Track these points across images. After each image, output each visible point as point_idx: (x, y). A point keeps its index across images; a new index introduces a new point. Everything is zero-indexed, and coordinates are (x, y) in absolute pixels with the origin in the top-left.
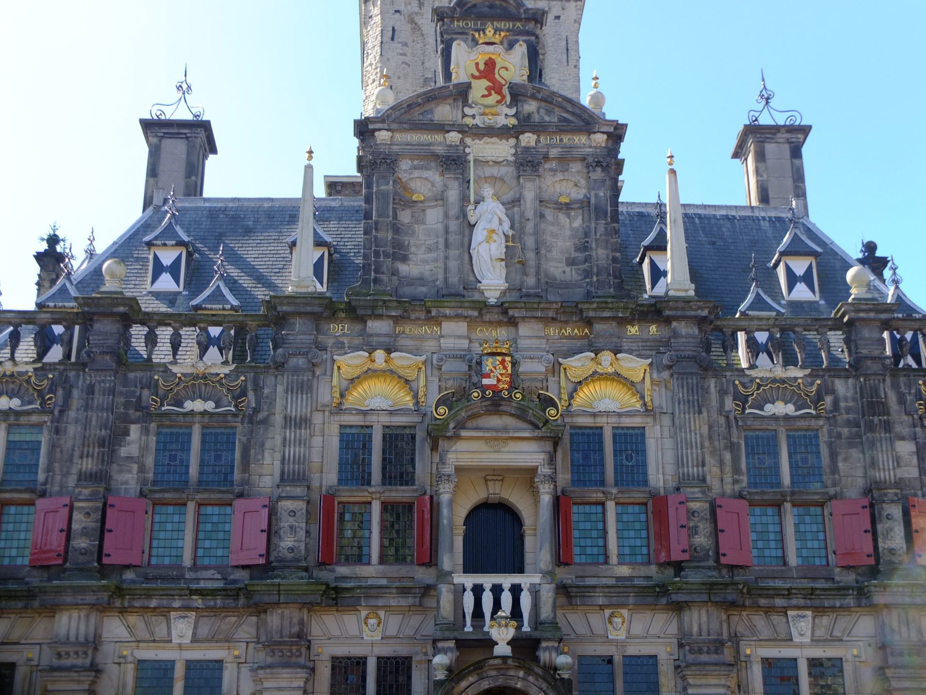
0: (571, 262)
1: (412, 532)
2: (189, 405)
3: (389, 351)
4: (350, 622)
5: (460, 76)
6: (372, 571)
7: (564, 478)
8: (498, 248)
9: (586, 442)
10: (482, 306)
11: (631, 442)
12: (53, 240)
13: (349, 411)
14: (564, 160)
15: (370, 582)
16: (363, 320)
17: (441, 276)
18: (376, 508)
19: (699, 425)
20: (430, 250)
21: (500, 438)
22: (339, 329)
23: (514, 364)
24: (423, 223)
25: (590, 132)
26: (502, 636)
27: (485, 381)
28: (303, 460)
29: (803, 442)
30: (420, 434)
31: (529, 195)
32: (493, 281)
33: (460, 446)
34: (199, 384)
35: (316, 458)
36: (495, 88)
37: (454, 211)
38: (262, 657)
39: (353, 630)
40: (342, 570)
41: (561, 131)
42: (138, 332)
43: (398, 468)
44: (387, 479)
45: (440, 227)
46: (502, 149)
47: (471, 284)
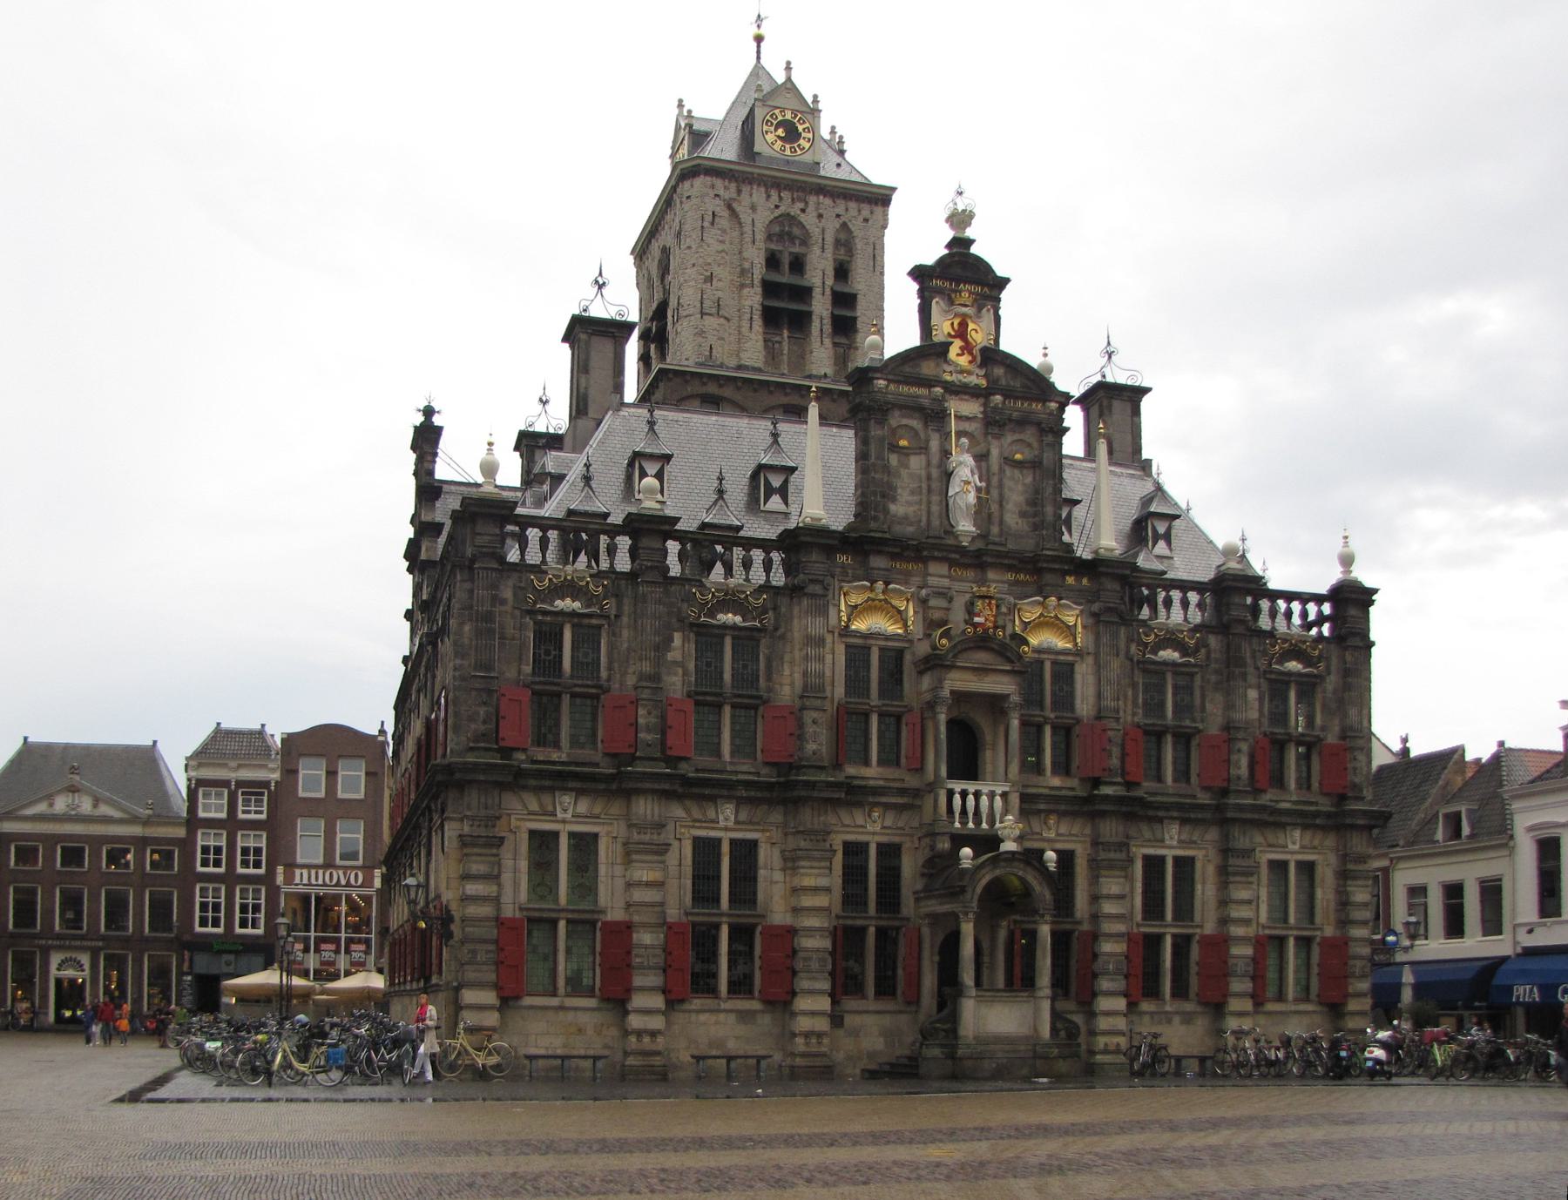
0: (1023, 514)
2: (720, 616)
3: (887, 583)
6: (873, 773)
8: (971, 498)
10: (962, 551)
12: (429, 412)
13: (857, 634)
14: (1022, 422)
15: (872, 783)
16: (866, 554)
17: (924, 519)
18: (874, 720)
20: (912, 493)
22: (842, 559)
23: (998, 607)
24: (907, 467)
25: (1045, 401)
27: (977, 619)
28: (821, 675)
30: (908, 657)
32: (965, 526)
33: (954, 675)
35: (828, 673)
37: (935, 460)
38: (792, 843)
39: (860, 821)
40: (851, 770)
41: (1024, 399)
44: (882, 694)
45: (923, 473)
46: (971, 408)
47: (950, 530)
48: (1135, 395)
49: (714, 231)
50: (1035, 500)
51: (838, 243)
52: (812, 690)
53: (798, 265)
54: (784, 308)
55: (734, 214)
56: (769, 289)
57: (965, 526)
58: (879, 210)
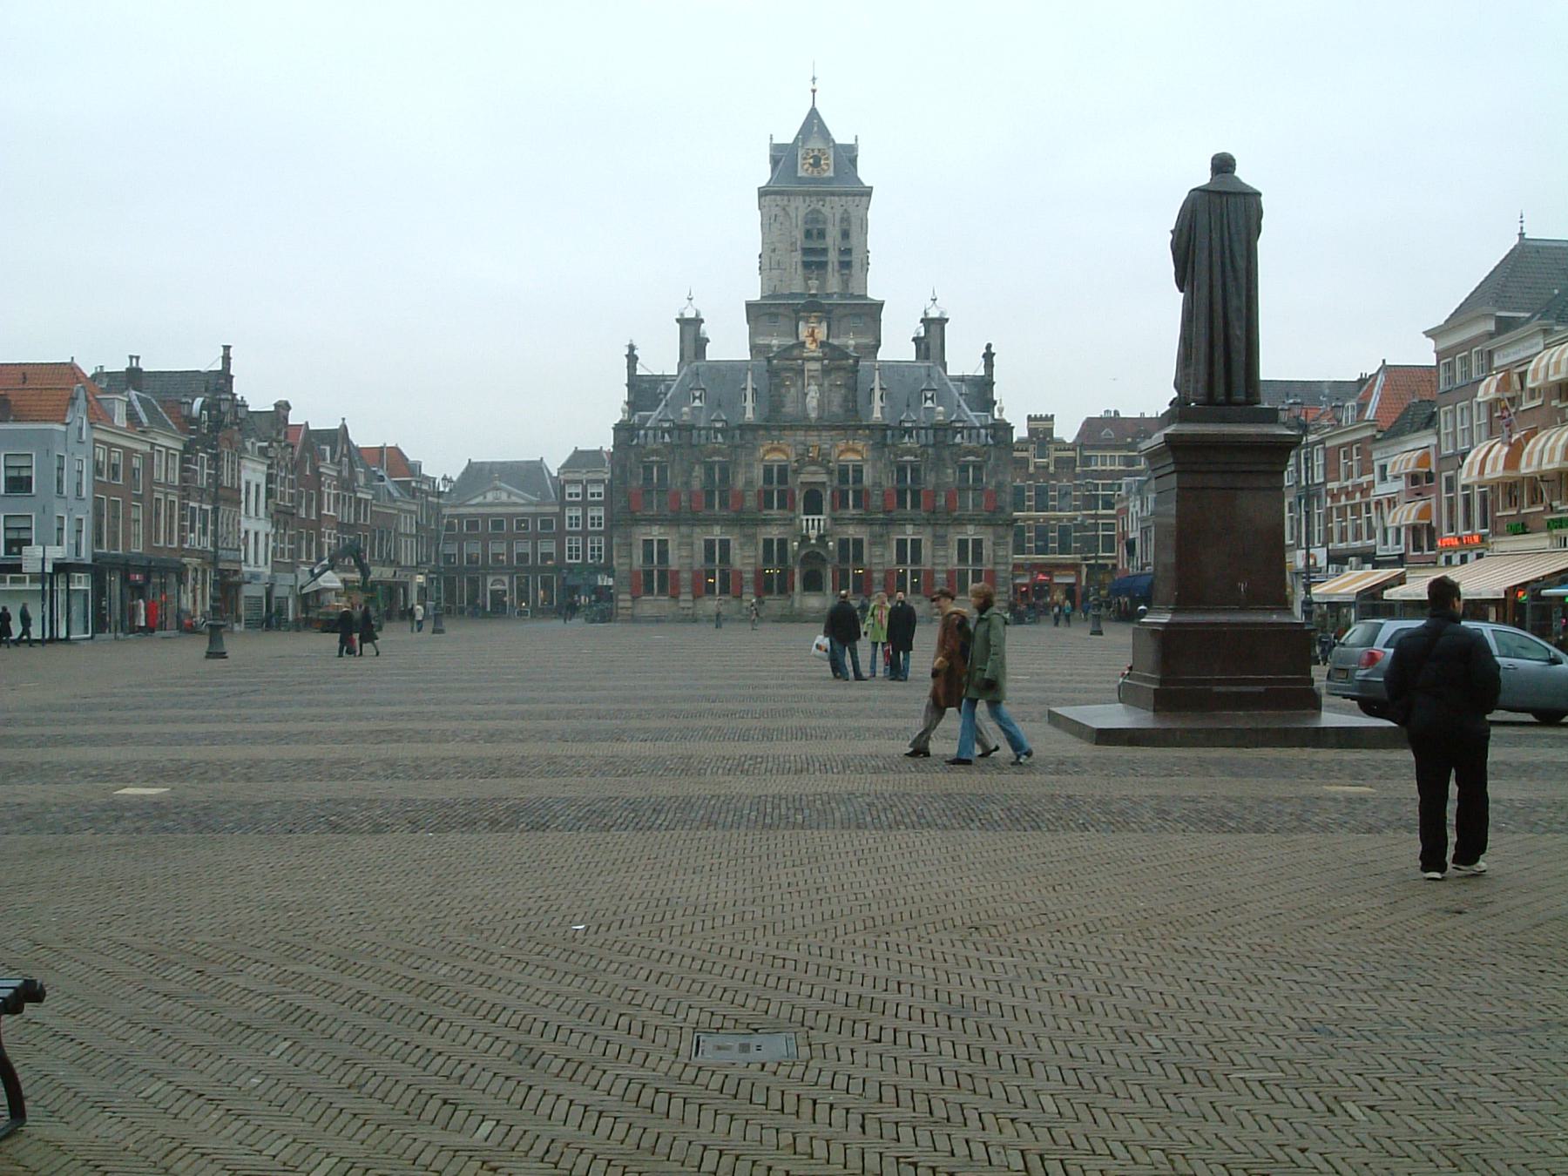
1: (786, 501)
4: (769, 529)
5: (802, 338)
7: (836, 482)
9: (843, 472)
11: (858, 470)
14: (839, 369)
19: (880, 465)
21: (815, 473)
26: (813, 533)
29: (915, 470)
31: (826, 384)
32: (813, 415)
34: (717, 452)
36: (815, 341)
42: (695, 432)
43: (783, 479)
46: (816, 366)
47: (807, 417)
48: (942, 321)
49: (777, 225)
50: (845, 399)
51: (842, 220)
52: (749, 483)
53: (822, 234)
54: (814, 262)
55: (787, 214)
56: (806, 251)
57: (813, 415)
58: (864, 199)
